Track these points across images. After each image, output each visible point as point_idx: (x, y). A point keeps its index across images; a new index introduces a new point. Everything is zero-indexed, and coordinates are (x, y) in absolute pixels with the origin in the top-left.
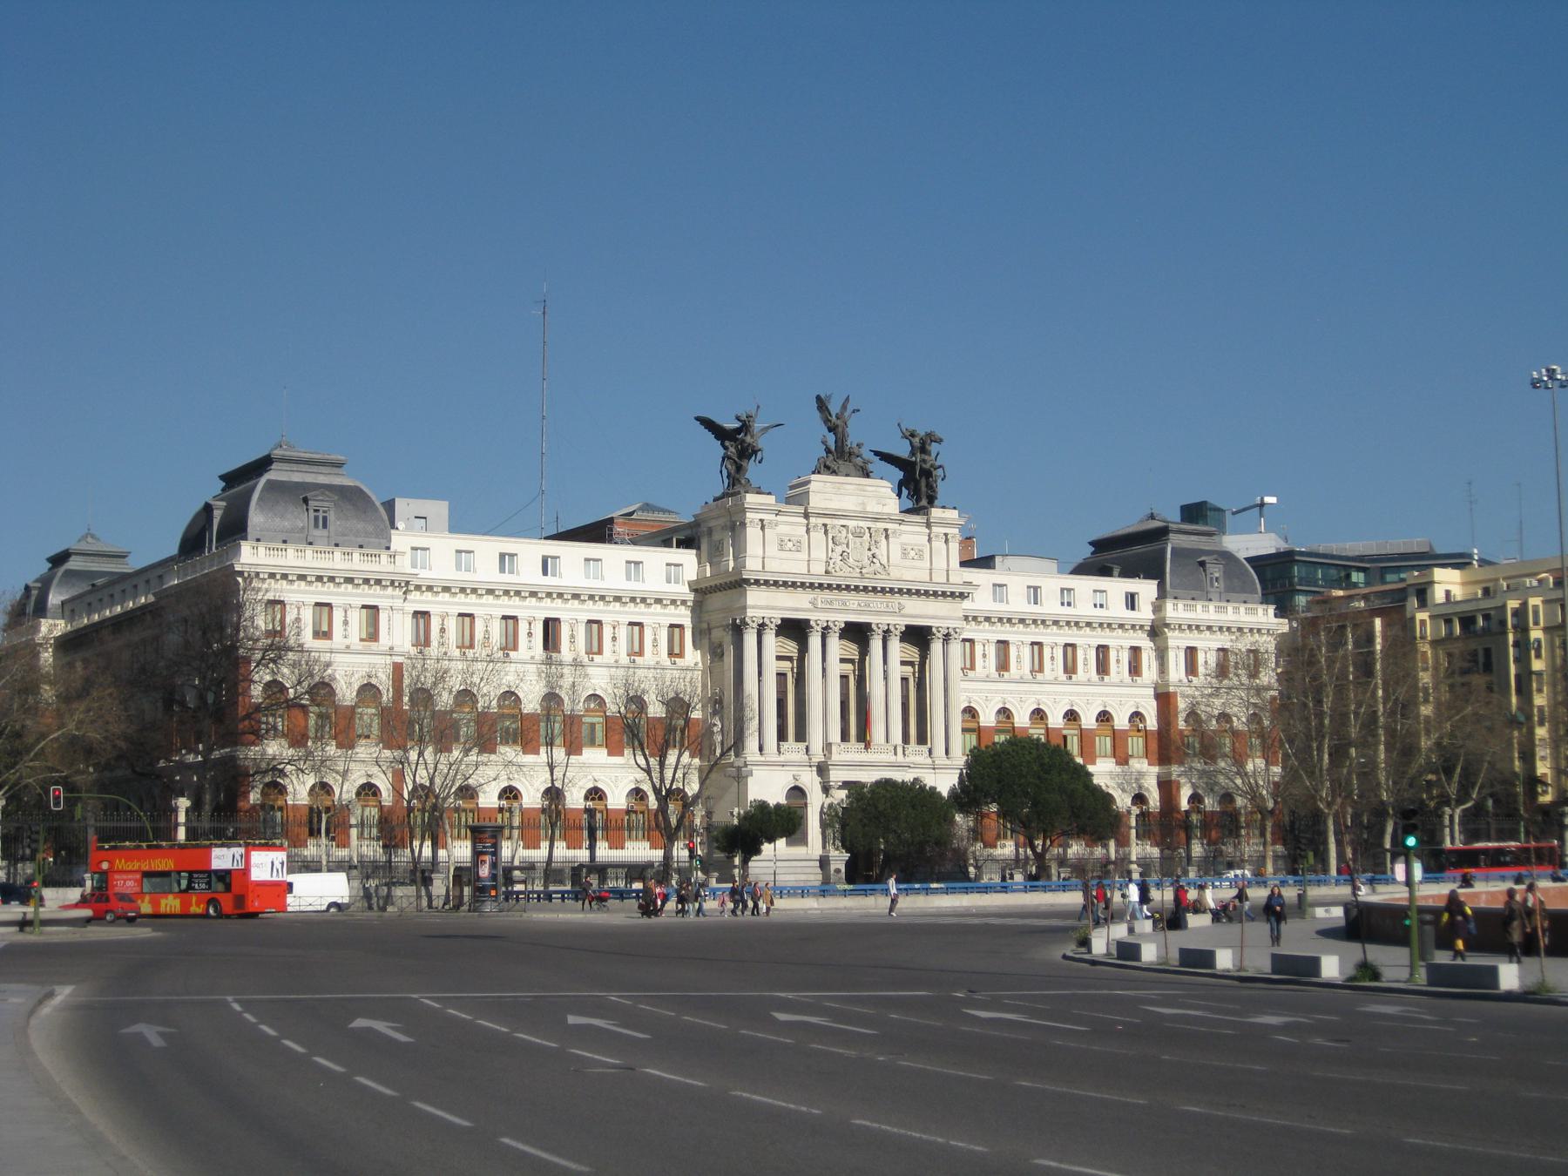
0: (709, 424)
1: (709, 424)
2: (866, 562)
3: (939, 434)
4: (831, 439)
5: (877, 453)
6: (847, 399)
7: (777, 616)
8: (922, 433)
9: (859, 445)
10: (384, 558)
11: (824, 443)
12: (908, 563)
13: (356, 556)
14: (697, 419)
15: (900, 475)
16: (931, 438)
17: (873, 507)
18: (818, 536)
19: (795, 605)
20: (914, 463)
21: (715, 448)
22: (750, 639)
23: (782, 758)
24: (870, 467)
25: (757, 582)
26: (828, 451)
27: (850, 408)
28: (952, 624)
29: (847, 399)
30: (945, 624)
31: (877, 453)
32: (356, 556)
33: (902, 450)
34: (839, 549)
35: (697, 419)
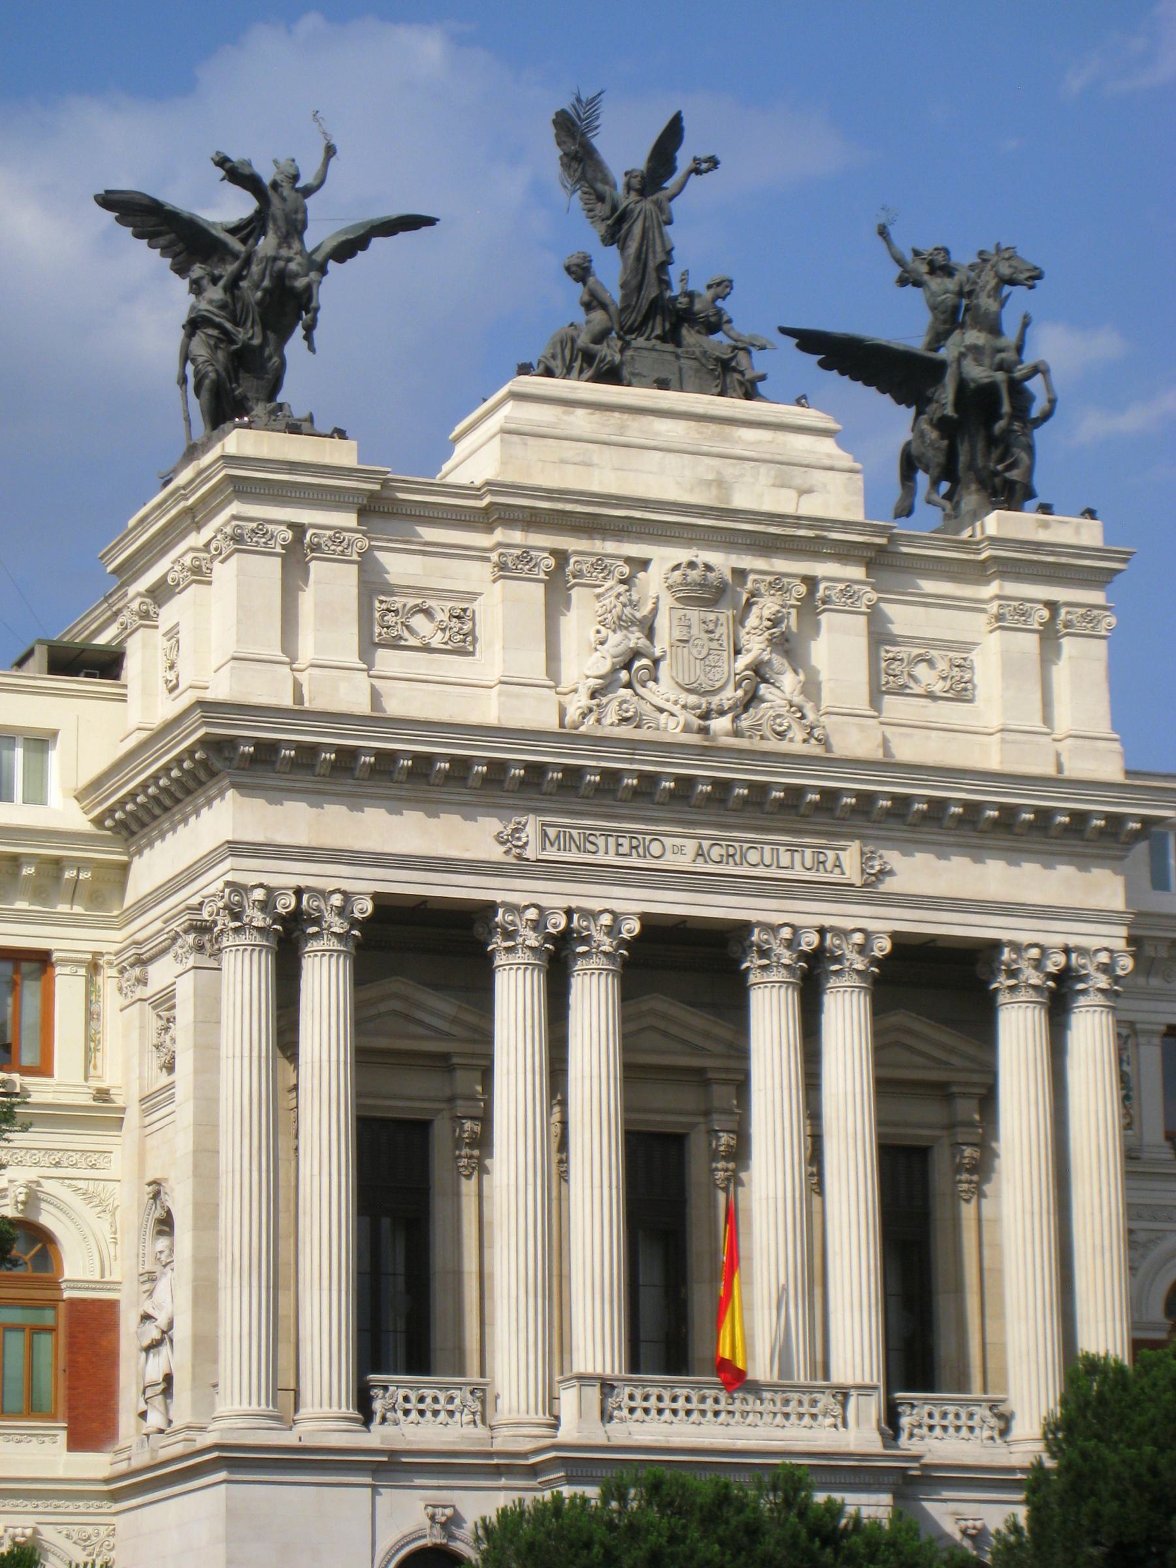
3: (1031, 255)
4: (610, 269)
5: (809, 341)
6: (673, 133)
7: (365, 885)
9: (723, 287)
11: (580, 271)
14: (108, 201)
15: (895, 424)
17: (756, 494)
20: (942, 366)
26: (593, 303)
27: (683, 160)
29: (673, 133)
30: (1056, 934)
31: (809, 341)
33: (903, 323)
35: (108, 201)
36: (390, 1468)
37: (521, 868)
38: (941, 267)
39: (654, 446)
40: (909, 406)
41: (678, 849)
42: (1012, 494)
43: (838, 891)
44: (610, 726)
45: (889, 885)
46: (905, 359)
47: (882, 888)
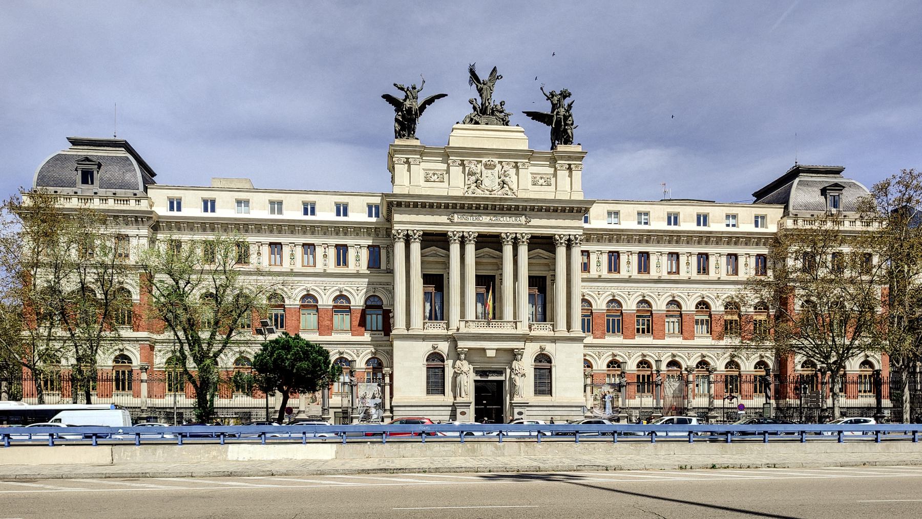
0: (388, 98)
1: (388, 98)
2: (497, 187)
5: (529, 114)
8: (558, 92)
10: (132, 202)
11: (471, 102)
12: (537, 188)
13: (111, 201)
14: (384, 97)
15: (548, 129)
16: (565, 95)
18: (456, 171)
19: (436, 222)
21: (390, 112)
22: (400, 247)
23: (426, 332)
24: (510, 118)
25: (399, 204)
26: (475, 108)
28: (573, 232)
31: (529, 114)
32: (111, 201)
33: (545, 108)
34: (473, 178)
35: (384, 97)
36: (425, 338)
37: (452, 223)
38: (552, 94)
39: (489, 136)
40: (548, 125)
41: (485, 219)
42: (568, 141)
43: (520, 225)
44: (470, 195)
45: (530, 224)
46: (547, 115)
47: (530, 224)
